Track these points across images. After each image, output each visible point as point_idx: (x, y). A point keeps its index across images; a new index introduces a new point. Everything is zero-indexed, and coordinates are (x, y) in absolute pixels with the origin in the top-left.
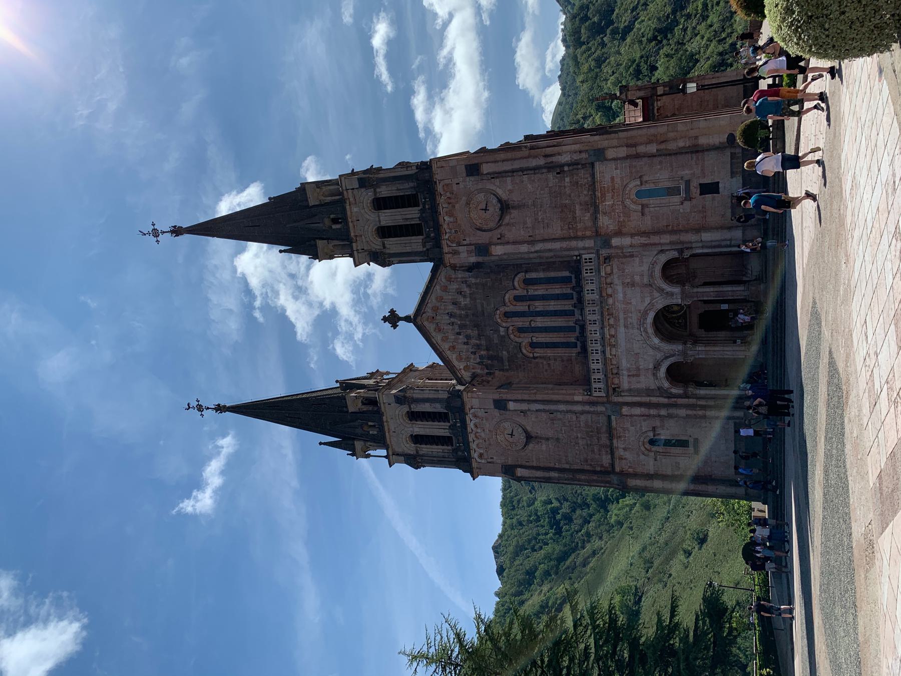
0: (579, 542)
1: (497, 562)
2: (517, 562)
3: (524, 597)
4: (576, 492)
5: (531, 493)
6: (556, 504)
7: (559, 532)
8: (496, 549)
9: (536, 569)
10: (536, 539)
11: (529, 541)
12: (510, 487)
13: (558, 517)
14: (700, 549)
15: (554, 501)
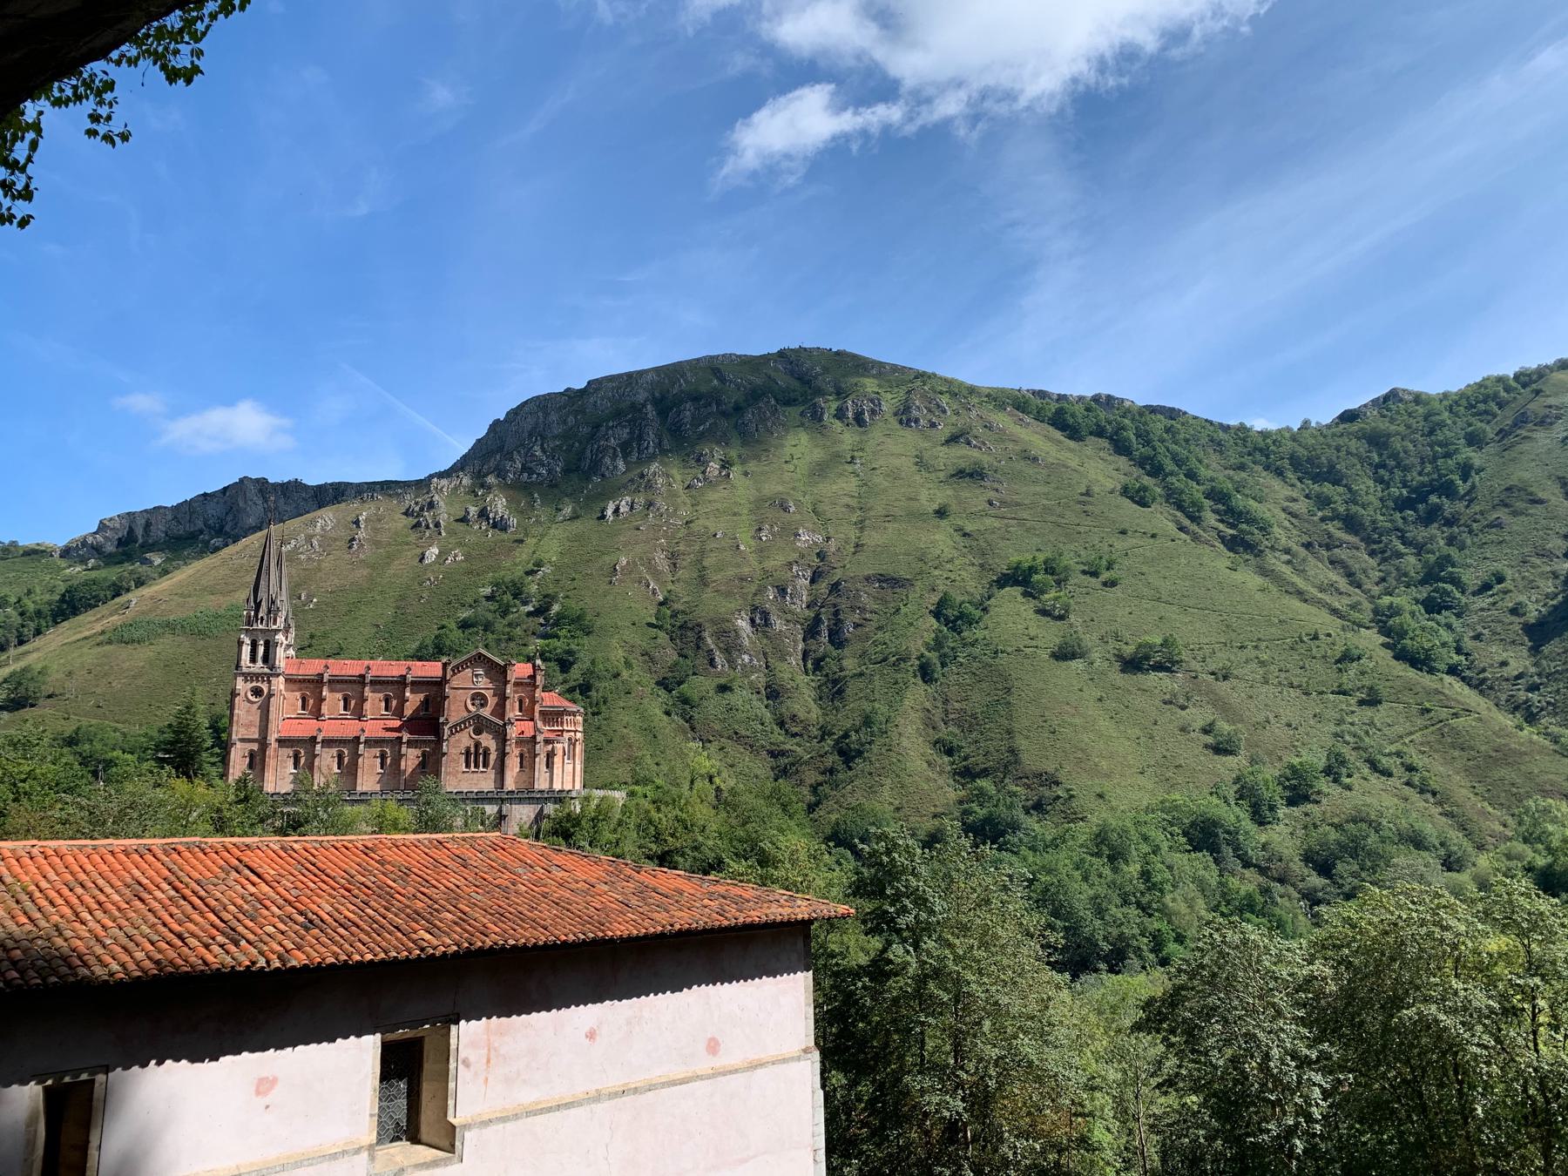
0: (1382, 545)
1: (1365, 406)
2: (1354, 445)
3: (1290, 475)
4: (1475, 521)
5: (1497, 435)
6: (1462, 488)
7: (1402, 505)
8: (1392, 396)
9: (1336, 483)
10: (1398, 465)
11: (1395, 456)
12: (1524, 386)
13: (1434, 499)
14: (1206, 746)
15: (1469, 484)
